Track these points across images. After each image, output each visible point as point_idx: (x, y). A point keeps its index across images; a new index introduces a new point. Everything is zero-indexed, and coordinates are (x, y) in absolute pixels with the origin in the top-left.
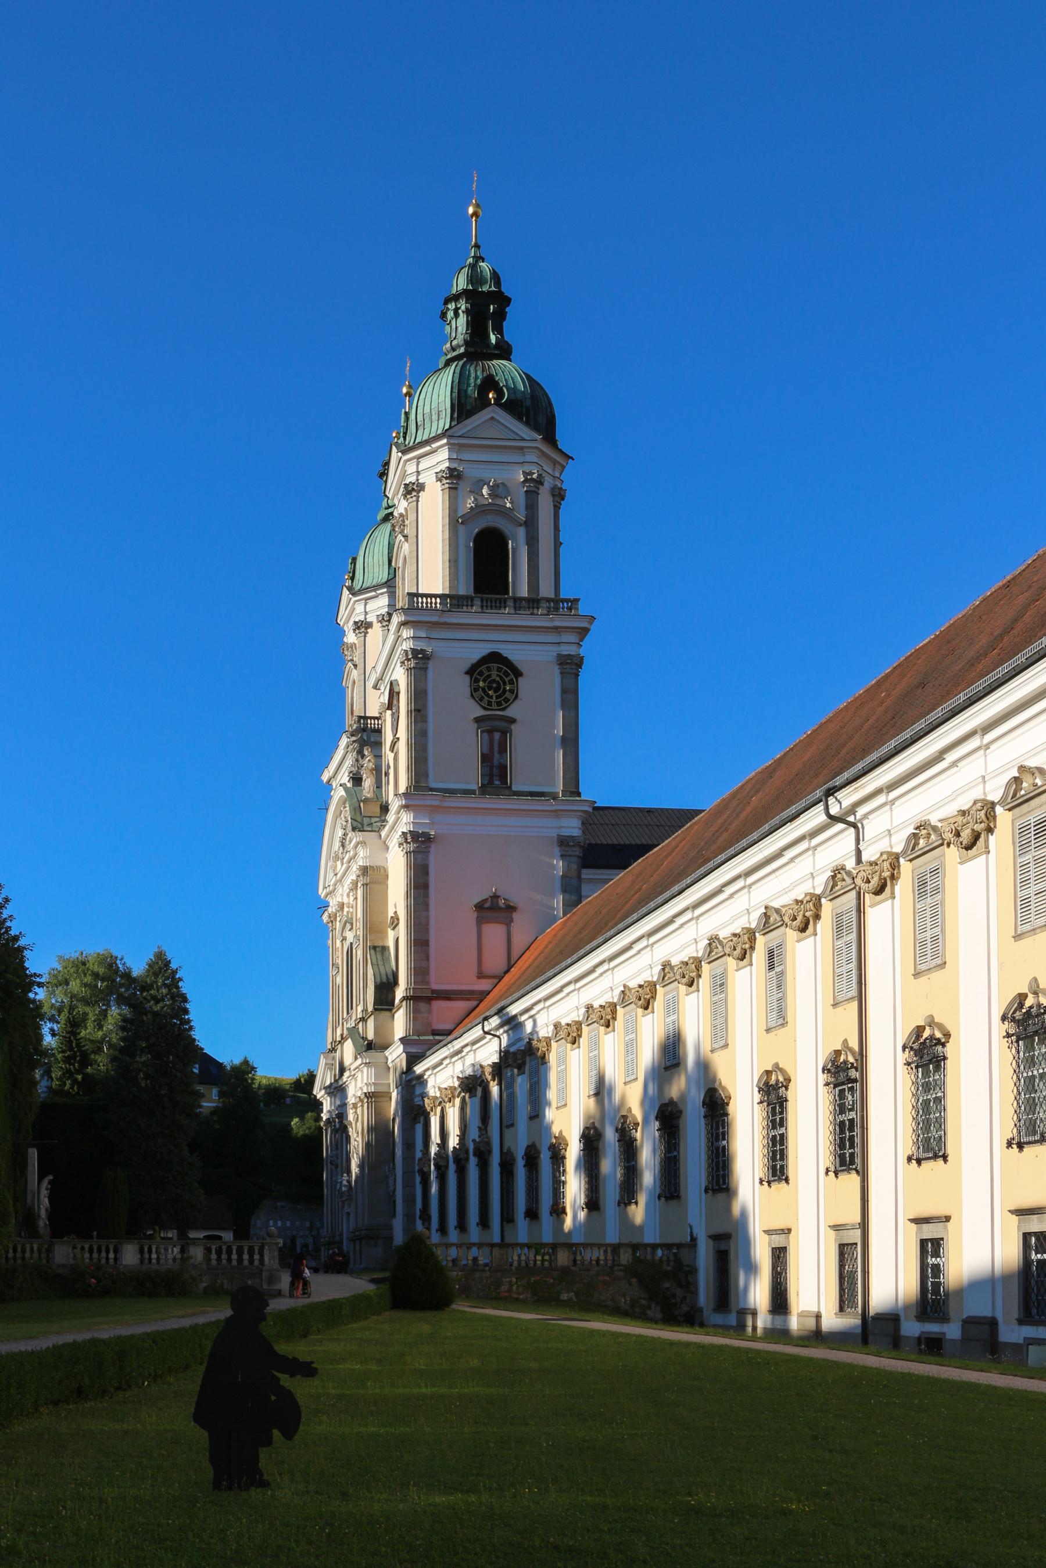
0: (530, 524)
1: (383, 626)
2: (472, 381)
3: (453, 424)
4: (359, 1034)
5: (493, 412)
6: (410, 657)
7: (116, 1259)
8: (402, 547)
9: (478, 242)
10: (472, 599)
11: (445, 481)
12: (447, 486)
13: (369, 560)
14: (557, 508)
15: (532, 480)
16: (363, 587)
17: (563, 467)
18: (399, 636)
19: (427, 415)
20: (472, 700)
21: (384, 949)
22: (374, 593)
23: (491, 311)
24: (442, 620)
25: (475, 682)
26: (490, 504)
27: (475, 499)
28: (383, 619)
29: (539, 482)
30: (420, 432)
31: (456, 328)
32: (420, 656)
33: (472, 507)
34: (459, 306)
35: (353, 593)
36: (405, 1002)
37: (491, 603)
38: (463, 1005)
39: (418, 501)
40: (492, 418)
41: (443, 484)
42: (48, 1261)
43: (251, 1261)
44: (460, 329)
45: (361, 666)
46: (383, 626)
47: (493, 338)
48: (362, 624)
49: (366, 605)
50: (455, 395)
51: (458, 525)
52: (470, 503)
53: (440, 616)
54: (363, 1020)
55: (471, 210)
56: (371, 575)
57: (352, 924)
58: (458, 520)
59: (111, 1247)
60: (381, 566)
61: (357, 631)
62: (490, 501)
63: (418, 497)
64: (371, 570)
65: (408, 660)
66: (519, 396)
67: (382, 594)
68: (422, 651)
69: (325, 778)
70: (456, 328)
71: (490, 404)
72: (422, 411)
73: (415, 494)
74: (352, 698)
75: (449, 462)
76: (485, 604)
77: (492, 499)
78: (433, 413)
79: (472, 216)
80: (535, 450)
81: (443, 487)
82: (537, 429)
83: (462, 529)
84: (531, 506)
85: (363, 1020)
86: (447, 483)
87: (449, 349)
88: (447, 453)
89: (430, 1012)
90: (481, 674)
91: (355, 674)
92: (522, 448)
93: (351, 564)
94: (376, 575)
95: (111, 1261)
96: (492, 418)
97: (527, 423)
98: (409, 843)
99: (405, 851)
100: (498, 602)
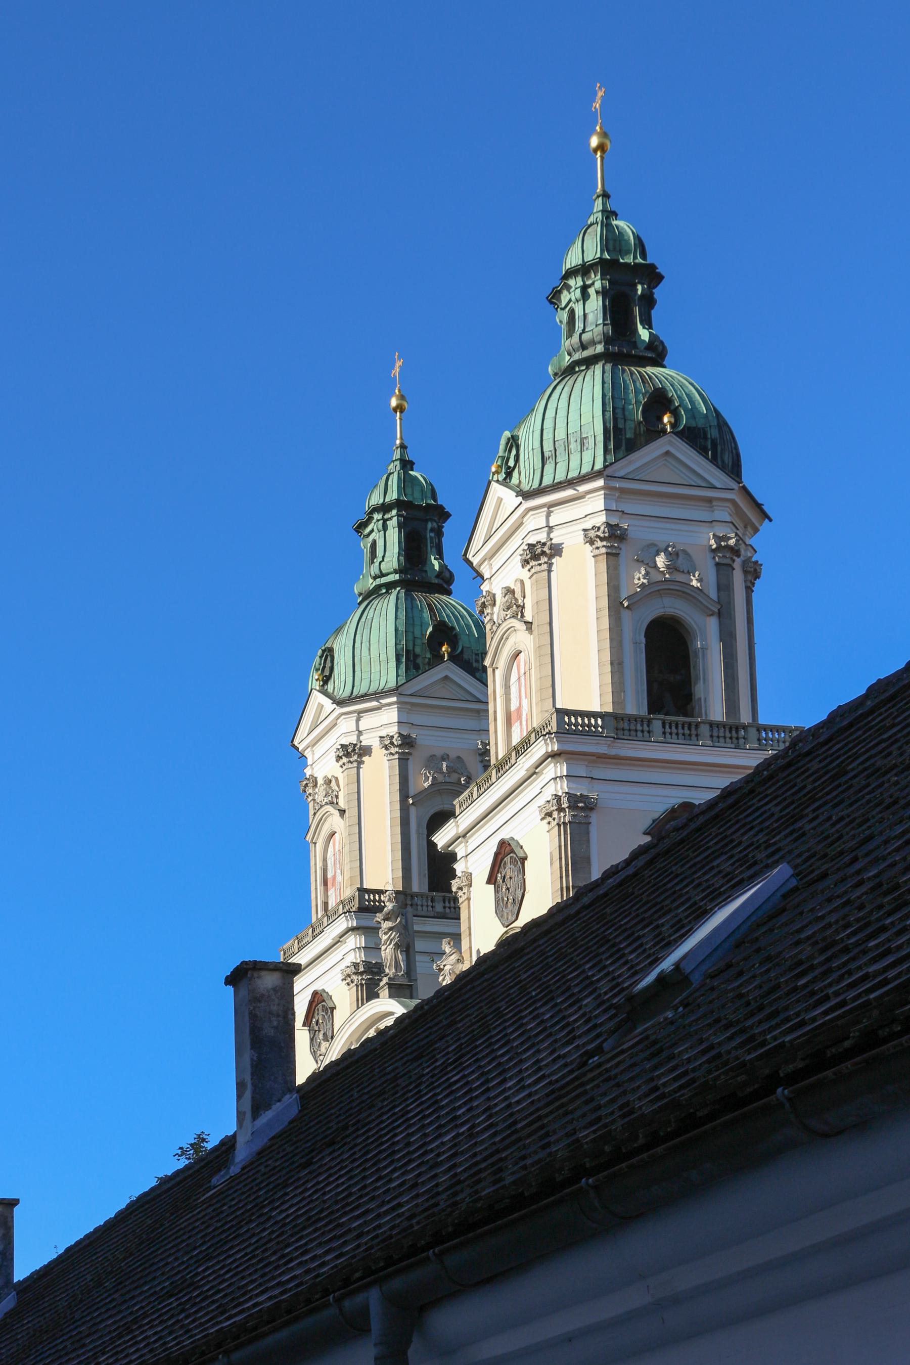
0: (724, 613)
1: (392, 754)
2: (632, 396)
3: (611, 458)
5: (668, 444)
6: (565, 805)
8: (507, 638)
9: (607, 189)
10: (649, 722)
11: (599, 543)
12: (604, 550)
13: (363, 653)
14: (749, 590)
15: (727, 546)
16: (355, 693)
17: (756, 530)
18: (535, 773)
19: (561, 442)
22: (374, 704)
23: (639, 292)
24: (613, 752)
26: (666, 580)
27: (647, 573)
28: (392, 743)
29: (735, 551)
30: (549, 468)
31: (585, 315)
32: (580, 805)
33: (643, 583)
34: (589, 282)
37: (677, 727)
39: (549, 571)
40: (668, 453)
41: (598, 548)
44: (590, 318)
45: (352, 813)
46: (392, 754)
47: (644, 334)
48: (354, 750)
49: (358, 720)
51: (622, 609)
52: (639, 577)
53: (609, 746)
55: (594, 141)
56: (366, 676)
58: (621, 603)
60: (383, 664)
62: (667, 576)
63: (551, 565)
64: (366, 668)
66: (701, 423)
67: (389, 704)
70: (585, 315)
71: (664, 431)
72: (551, 436)
73: (546, 559)
74: (325, 860)
75: (606, 514)
76: (668, 730)
77: (670, 574)
78: (572, 440)
79: (595, 151)
80: (728, 504)
81: (597, 552)
82: (723, 468)
83: (626, 615)
84: (725, 587)
86: (604, 546)
87: (576, 346)
88: (602, 501)
92: (709, 500)
93: (321, 657)
94: (375, 677)
96: (668, 453)
97: (714, 461)
100: (686, 728)
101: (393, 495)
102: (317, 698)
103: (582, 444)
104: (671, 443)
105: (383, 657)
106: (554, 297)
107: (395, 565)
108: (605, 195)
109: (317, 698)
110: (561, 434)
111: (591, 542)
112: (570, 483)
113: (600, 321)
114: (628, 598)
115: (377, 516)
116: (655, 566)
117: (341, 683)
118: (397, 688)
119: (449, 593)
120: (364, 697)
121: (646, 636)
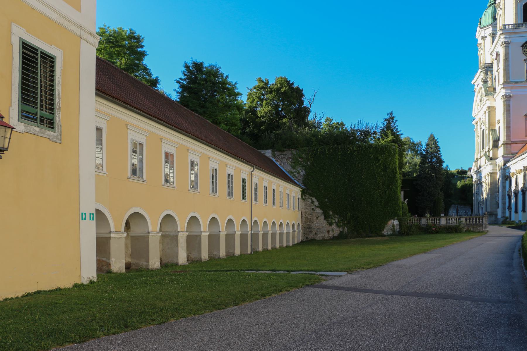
4: (487, 155)
7: (439, 223)
10: (523, 24)
13: (486, 18)
20: (523, 54)
21: (495, 130)
22: (487, 28)
24: (514, 31)
25: (524, 49)
35: (481, 28)
36: (503, 145)
38: (521, 145)
42: (419, 223)
43: (479, 222)
45: (484, 49)
49: (485, 31)
54: (489, 151)
56: (486, 22)
57: (484, 124)
59: (438, 219)
61: (482, 39)
64: (486, 21)
65: (503, 44)
68: (507, 41)
69: (472, 83)
74: (481, 59)
83: (519, 4)
85: (489, 151)
89: (511, 148)
90: (526, 46)
91: (482, 52)
94: (488, 22)
95: (438, 223)
98: (504, 98)
99: (503, 101)
102: (478, 28)
105: (489, 18)
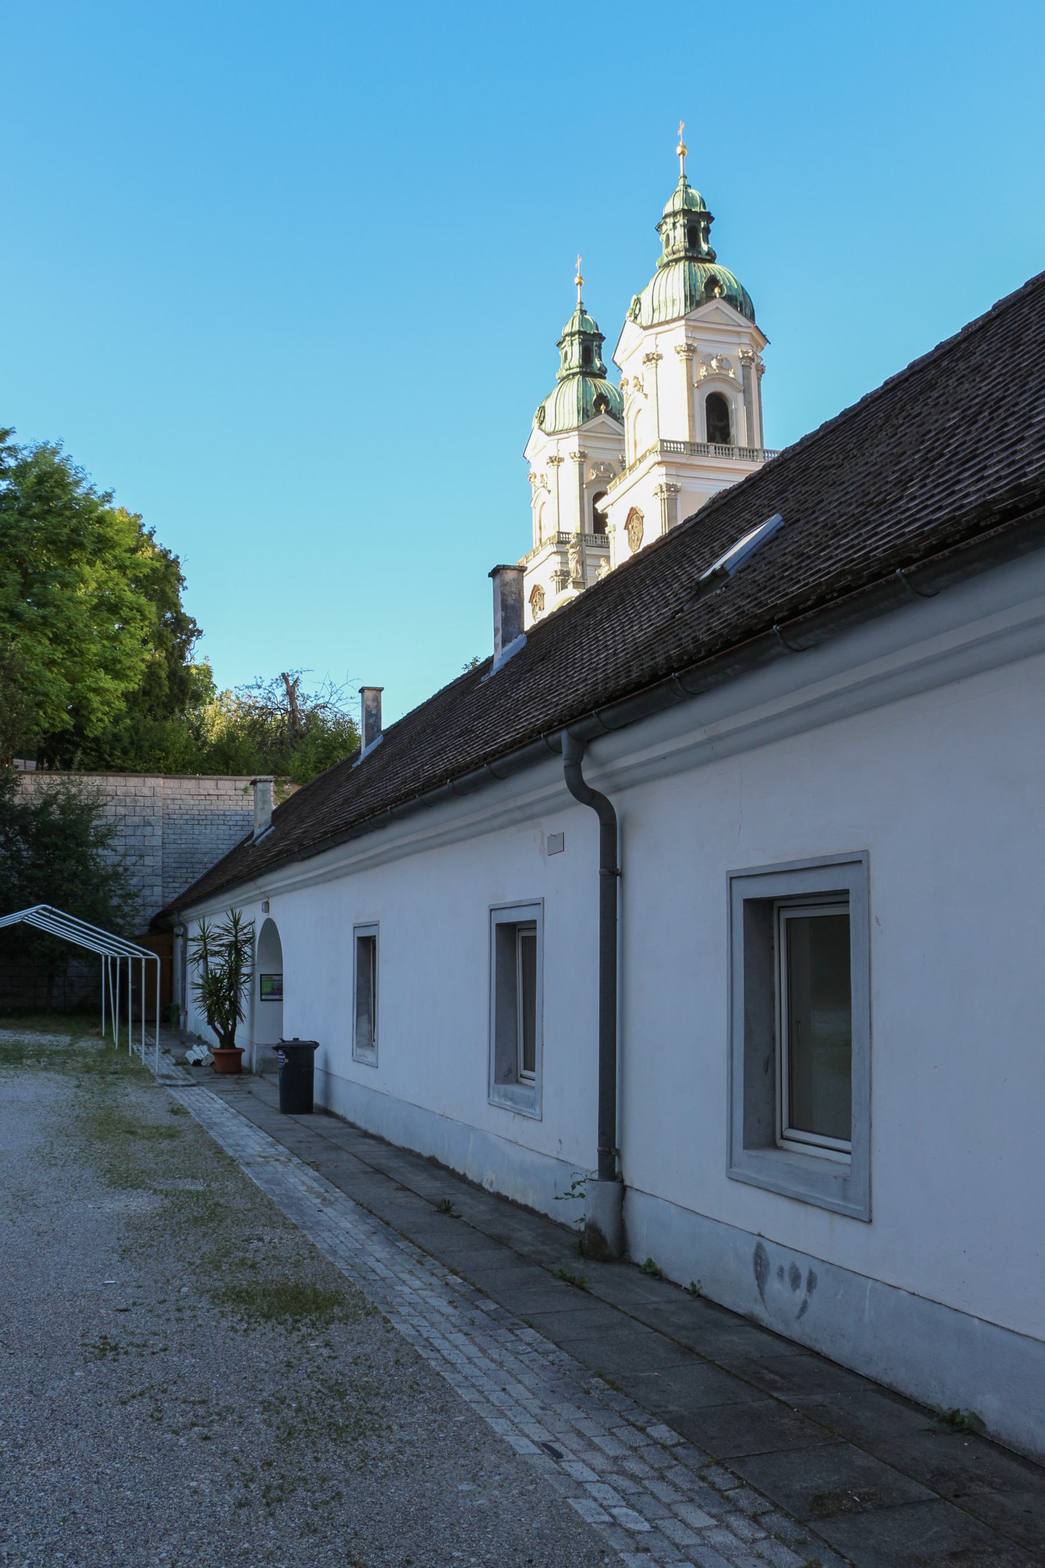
0: (746, 391)
2: (699, 278)
3: (688, 310)
6: (664, 489)
11: (682, 353)
13: (560, 408)
14: (759, 379)
15: (748, 357)
17: (763, 349)
23: (702, 226)
24: (689, 462)
27: (707, 370)
29: (752, 359)
30: (656, 313)
40: (717, 308)
44: (677, 239)
45: (554, 492)
47: (705, 247)
50: (688, 288)
52: (703, 372)
55: (679, 150)
66: (734, 293)
68: (674, 486)
71: (715, 297)
82: (745, 316)
83: (696, 391)
84: (746, 378)
92: (739, 333)
97: (741, 312)
101: (576, 328)
102: (537, 434)
103: (673, 303)
104: (718, 303)
106: (659, 228)
107: (577, 364)
108: (685, 177)
109: (537, 434)
110: (662, 298)
111: (678, 353)
112: (667, 322)
113: (683, 240)
114: (697, 382)
115: (568, 338)
116: (711, 366)
117: (548, 425)
118: (578, 427)
119: (605, 378)
120: (561, 432)
121: (707, 401)
